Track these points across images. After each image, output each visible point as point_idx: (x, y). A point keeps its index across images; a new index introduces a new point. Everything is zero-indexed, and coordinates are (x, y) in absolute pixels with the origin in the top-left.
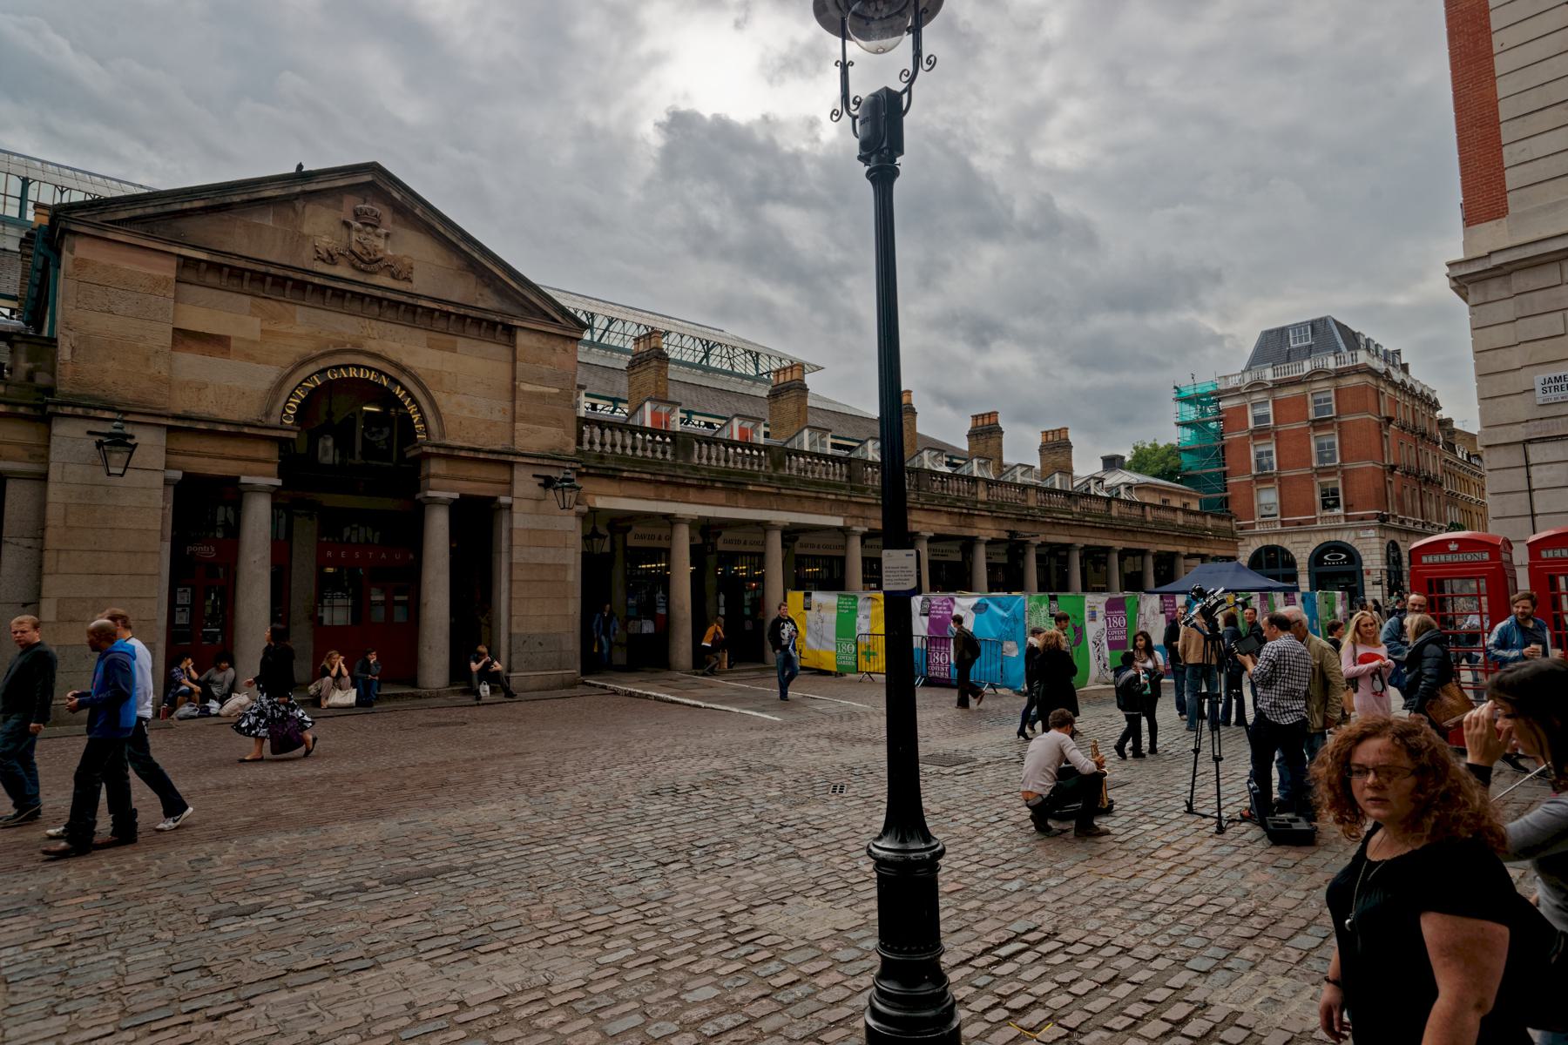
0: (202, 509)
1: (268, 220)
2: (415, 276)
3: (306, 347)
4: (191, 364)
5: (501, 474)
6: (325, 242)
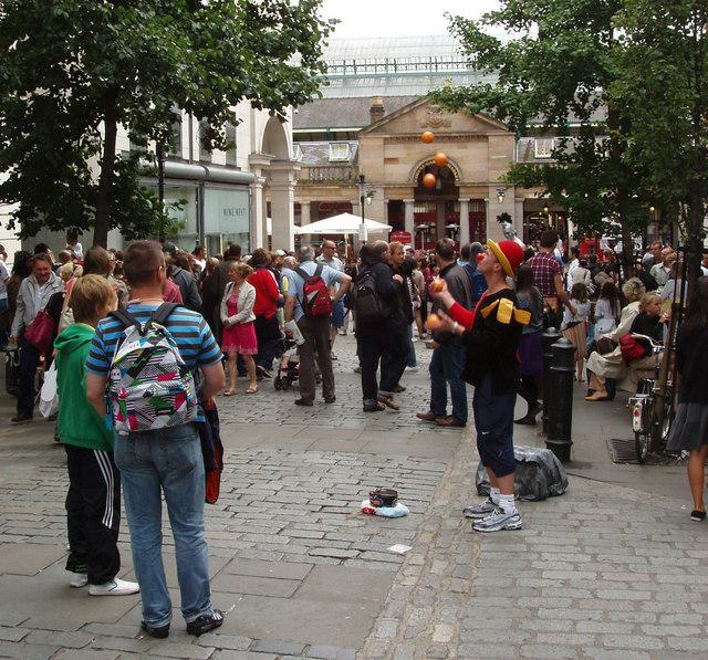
0: (395, 212)
1: (407, 119)
2: (453, 124)
3: (418, 157)
4: (390, 168)
5: (484, 190)
6: (423, 121)
